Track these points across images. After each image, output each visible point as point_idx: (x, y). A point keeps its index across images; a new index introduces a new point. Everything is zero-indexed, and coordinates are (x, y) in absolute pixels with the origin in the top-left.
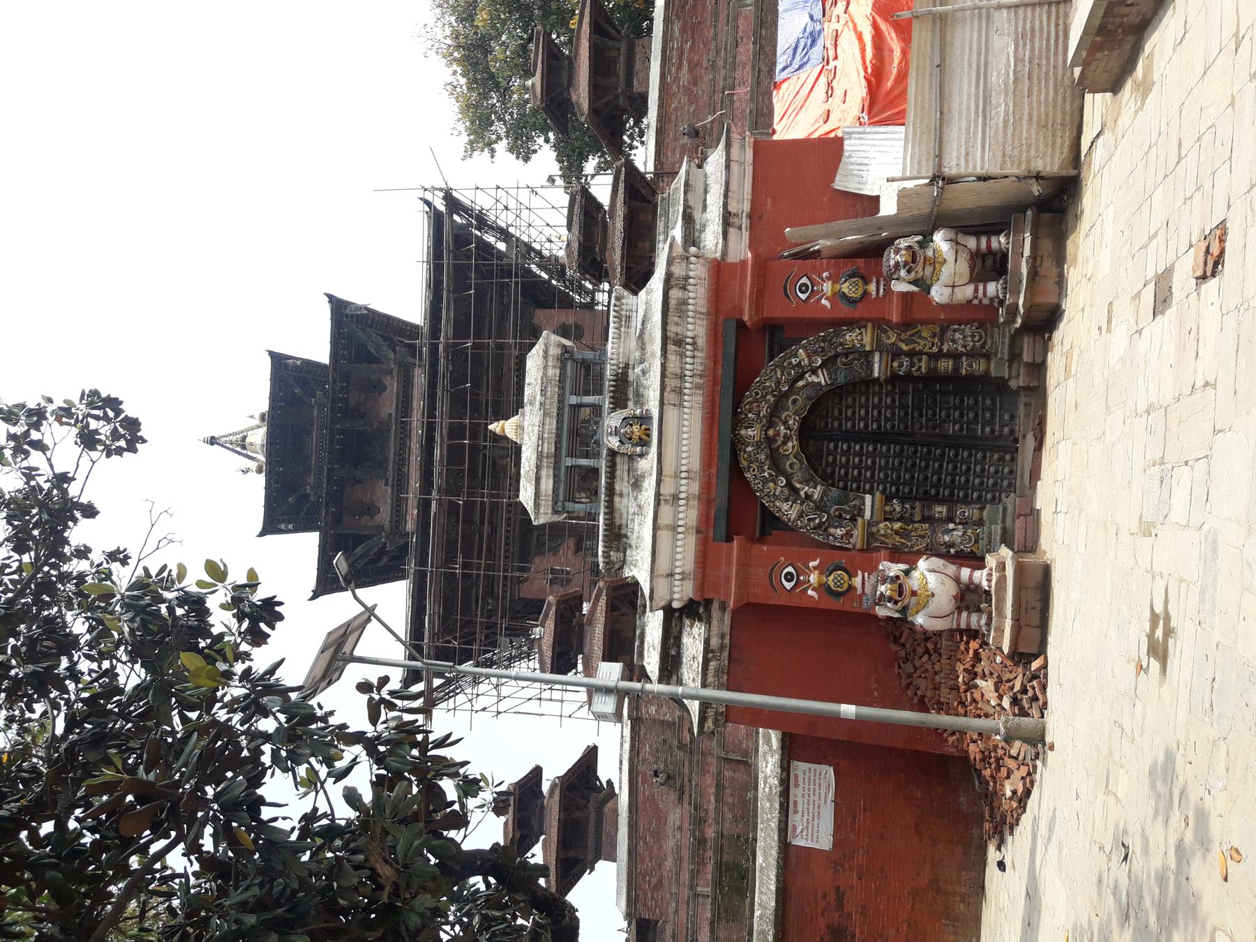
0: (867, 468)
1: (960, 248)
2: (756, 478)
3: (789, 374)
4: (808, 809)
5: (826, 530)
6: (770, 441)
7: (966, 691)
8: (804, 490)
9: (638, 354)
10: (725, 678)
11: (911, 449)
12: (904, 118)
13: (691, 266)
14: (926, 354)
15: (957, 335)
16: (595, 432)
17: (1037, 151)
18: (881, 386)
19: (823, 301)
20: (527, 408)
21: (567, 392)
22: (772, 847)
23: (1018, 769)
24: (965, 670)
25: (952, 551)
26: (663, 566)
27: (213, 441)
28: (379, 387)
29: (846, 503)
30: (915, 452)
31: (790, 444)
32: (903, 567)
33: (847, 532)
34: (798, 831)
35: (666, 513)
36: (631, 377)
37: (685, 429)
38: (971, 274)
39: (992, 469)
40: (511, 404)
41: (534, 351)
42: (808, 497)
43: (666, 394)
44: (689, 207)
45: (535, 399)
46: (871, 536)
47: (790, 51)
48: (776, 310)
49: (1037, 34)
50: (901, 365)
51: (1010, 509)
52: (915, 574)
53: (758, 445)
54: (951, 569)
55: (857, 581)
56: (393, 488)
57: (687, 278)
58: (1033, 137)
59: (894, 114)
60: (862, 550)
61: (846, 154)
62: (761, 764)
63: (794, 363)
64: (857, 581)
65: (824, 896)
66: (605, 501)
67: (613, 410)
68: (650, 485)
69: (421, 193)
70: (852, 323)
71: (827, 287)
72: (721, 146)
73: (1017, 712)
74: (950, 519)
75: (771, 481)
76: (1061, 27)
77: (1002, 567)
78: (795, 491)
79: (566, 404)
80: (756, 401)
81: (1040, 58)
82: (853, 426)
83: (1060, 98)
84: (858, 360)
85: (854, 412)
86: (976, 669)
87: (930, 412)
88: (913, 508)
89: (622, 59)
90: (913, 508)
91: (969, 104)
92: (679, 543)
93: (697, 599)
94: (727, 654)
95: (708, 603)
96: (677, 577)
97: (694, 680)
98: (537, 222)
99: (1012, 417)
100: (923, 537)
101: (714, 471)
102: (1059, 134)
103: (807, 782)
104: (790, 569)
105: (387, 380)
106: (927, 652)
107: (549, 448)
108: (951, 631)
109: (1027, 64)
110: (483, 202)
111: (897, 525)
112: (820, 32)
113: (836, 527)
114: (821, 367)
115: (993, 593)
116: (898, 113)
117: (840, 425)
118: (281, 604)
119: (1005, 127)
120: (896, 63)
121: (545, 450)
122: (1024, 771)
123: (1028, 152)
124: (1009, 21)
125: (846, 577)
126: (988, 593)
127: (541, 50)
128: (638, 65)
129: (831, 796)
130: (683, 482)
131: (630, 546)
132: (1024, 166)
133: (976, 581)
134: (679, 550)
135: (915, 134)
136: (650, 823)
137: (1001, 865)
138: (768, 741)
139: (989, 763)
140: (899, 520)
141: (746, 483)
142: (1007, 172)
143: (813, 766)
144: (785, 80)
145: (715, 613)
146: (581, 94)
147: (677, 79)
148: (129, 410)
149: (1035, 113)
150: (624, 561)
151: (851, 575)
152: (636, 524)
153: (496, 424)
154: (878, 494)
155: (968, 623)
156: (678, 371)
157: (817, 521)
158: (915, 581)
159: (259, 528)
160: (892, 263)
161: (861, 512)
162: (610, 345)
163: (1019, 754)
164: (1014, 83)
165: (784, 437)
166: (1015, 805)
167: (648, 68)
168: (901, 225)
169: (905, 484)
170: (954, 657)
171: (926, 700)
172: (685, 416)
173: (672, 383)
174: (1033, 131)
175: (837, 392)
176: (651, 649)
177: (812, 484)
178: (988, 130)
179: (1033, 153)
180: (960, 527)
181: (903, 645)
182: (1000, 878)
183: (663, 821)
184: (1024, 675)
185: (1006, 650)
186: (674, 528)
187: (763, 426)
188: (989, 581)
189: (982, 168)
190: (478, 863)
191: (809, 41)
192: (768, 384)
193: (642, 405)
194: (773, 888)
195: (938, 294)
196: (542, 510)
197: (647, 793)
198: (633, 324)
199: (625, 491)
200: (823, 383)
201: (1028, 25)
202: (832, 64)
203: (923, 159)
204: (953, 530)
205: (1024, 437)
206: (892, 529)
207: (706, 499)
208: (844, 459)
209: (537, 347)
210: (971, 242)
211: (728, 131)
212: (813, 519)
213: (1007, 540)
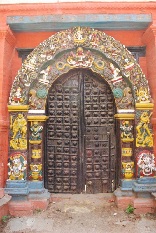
18: (111, 115)
31: (73, 62)
33: (19, 99)
46: (16, 114)
50: (127, 126)
53: (71, 42)
60: (7, 109)
63: (125, 60)
74: (31, 161)
78: (44, 68)
80: (100, 39)
90: (38, 138)
114: (124, 78)
141: (47, 37)
154: (45, 117)
157: (25, 80)
165: (78, 58)
200: (113, 80)
212: (26, 79)
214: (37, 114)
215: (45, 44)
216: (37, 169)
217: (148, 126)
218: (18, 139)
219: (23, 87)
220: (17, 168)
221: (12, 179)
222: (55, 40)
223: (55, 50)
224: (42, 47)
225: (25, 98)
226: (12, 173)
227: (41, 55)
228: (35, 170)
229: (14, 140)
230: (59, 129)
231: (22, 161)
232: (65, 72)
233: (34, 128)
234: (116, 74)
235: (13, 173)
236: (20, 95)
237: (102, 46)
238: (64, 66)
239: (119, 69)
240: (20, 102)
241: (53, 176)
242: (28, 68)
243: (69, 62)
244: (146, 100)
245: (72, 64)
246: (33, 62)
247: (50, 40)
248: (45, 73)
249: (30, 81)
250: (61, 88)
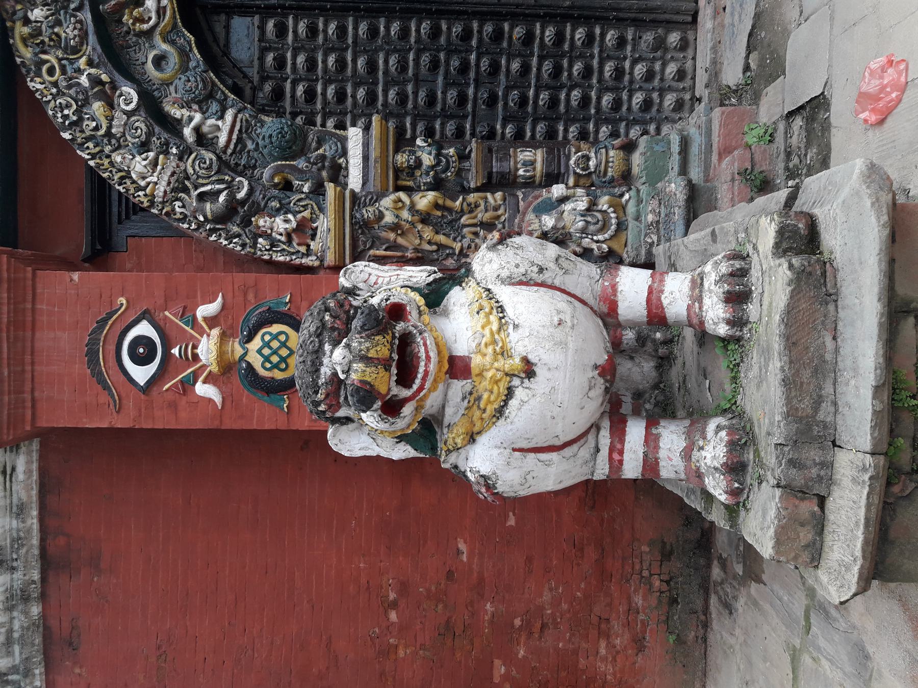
10: (35, 610)
11: (457, 29)
29: (302, 152)
30: (466, 35)
32: (420, 275)
74: (552, 178)
88: (463, 157)
90: (463, 157)
104: (144, 329)
111: (424, 201)
155: (651, 464)
157: (222, 198)
161: (338, 173)
169: (446, 116)
177: (214, 107)
180: (580, 191)
204: (563, 200)
206: (412, 208)
214: (366, 158)
215: (66, 117)
216: (588, 158)
218: (465, 230)
219: (250, 208)
220: (579, 218)
221: (626, 246)
222: (51, 72)
223: (93, 71)
224: (82, 131)
225: (299, 200)
226: (597, 242)
227: (114, 131)
228: (592, 163)
229: (466, 245)
230: (431, 100)
232: (194, 45)
233: (424, 167)
235: (601, 237)
236: (287, 221)
238: (165, 47)
240: (313, 220)
241: (624, 123)
242: (169, 183)
243: (148, 22)
245: (158, 12)
246: (144, 163)
247: (50, 97)
248: (193, 124)
249: (227, 178)
250: (261, 90)
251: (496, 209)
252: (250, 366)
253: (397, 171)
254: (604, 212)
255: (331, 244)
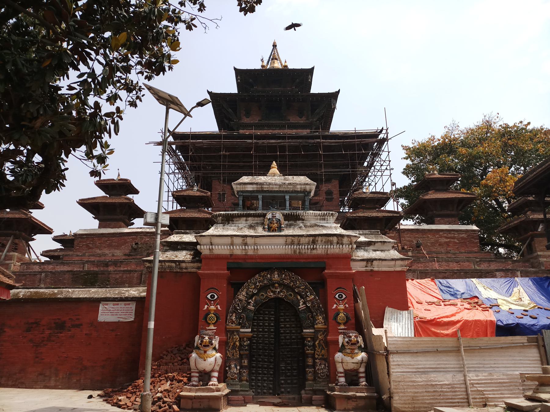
0: (263, 329)
1: (359, 365)
2: (256, 280)
3: (303, 292)
4: (115, 310)
5: (234, 312)
6: (273, 285)
7: (165, 377)
8: (252, 302)
9: (308, 224)
10: (168, 271)
12: (418, 336)
13: (347, 246)
14: (314, 352)
15: (323, 366)
16: (274, 208)
17: (402, 396)
19: (335, 305)
20: (283, 178)
21: (290, 195)
22: (98, 295)
23: (130, 402)
24: (174, 376)
25: (227, 368)
26: (216, 240)
27: (275, 46)
28: (301, 114)
29: (247, 321)
30: (271, 350)
31: (272, 294)
32: (217, 347)
34: (106, 306)
35: (239, 241)
36: (298, 222)
37: (276, 247)
38: (348, 370)
39: (265, 384)
40: (284, 170)
41: (308, 179)
42: (249, 303)
43: (291, 237)
44: (375, 244)
45: (287, 181)
46: (232, 332)
47: (448, 285)
48: (331, 284)
49: (454, 394)
50: (309, 342)
51: (247, 393)
52: (214, 352)
54: (217, 368)
55: (212, 327)
56: (257, 123)
57: (342, 244)
58: (408, 394)
59: (419, 332)
60: (226, 328)
61: (401, 312)
62: (134, 289)
64: (212, 327)
65: (78, 319)
66: (243, 213)
67: (283, 215)
68: (252, 233)
69: (385, 128)
70: (326, 319)
71: (342, 307)
72: (402, 256)
73: (155, 400)
74: (242, 367)
75: (255, 286)
76: (457, 404)
77: (218, 390)
79: (286, 194)
81: (443, 395)
82: (282, 322)
83: (426, 405)
84: (310, 322)
85: (288, 322)
86: (174, 381)
87: (289, 356)
88: (246, 350)
89: (449, 212)
90: (246, 350)
91: (421, 365)
92: (226, 247)
93: (201, 256)
94: (179, 271)
95: (200, 261)
96: (211, 247)
97: (167, 257)
98: (377, 179)
99: (289, 392)
100: (233, 355)
101: (258, 261)
102: (410, 406)
103: (127, 309)
104: (216, 297)
105: (304, 118)
106: (182, 359)
107: (266, 188)
108: (190, 369)
109: (440, 390)
110: (384, 156)
111: (238, 343)
112: (456, 297)
113: (236, 316)
115: (207, 387)
116: (420, 334)
117: (282, 316)
118: (164, 74)
119: (412, 381)
120: (442, 332)
121: (264, 186)
122: (129, 404)
123: (401, 392)
124: (459, 381)
125: (213, 322)
126: (207, 385)
127: (450, 177)
128: (446, 219)
129: (121, 320)
130: (253, 247)
131: (224, 226)
132: (395, 391)
133: (212, 379)
134: (223, 247)
135: (406, 341)
136: (115, 242)
137: (90, 397)
138: (143, 291)
139: (134, 389)
140: (240, 344)
142: (392, 383)
143: (134, 311)
144: (435, 283)
145: (196, 265)
146: (432, 195)
147: (441, 237)
148: (258, 8)
149: (418, 395)
150: (218, 223)
151: (214, 324)
152: (234, 228)
153: (276, 164)
154: (251, 334)
155: (194, 376)
156: (301, 242)
157: (238, 308)
158: (211, 352)
159: (238, 67)
160: (351, 334)
161: (243, 327)
162: (312, 212)
163: (136, 401)
164: (432, 384)
166: (115, 401)
167: (445, 224)
168: (368, 338)
170: (180, 371)
171: (161, 360)
172: (281, 247)
173: (296, 240)
174: (411, 394)
175: (296, 313)
176: (180, 237)
178: (410, 374)
179: (401, 394)
180: (238, 371)
181: (185, 349)
182: (85, 397)
183: (116, 248)
184: (171, 402)
185: (181, 394)
186: (232, 244)
187: (279, 281)
188: (212, 385)
189: (393, 372)
190: (49, 163)
191: (453, 293)
192: (298, 282)
193: (286, 227)
194: (81, 296)
195: (339, 356)
196: (238, 186)
197: (128, 240)
198: (321, 222)
199: (248, 222)
201: (458, 390)
202: (442, 304)
203: (396, 346)
204: (237, 368)
205: (280, 398)
206: (236, 341)
207: (246, 257)
208: (267, 318)
209: (309, 180)
210: (362, 369)
211: (408, 259)
213: (233, 392)
217: (323, 342)
222: (259, 278)
228: (244, 374)
231: (236, 367)
234: (301, 303)
236: (234, 319)
237: (292, 283)
239: (304, 300)
244: (322, 323)
251: (236, 356)
252: (209, 314)
253: (244, 338)
254: (234, 376)
255: (230, 327)
